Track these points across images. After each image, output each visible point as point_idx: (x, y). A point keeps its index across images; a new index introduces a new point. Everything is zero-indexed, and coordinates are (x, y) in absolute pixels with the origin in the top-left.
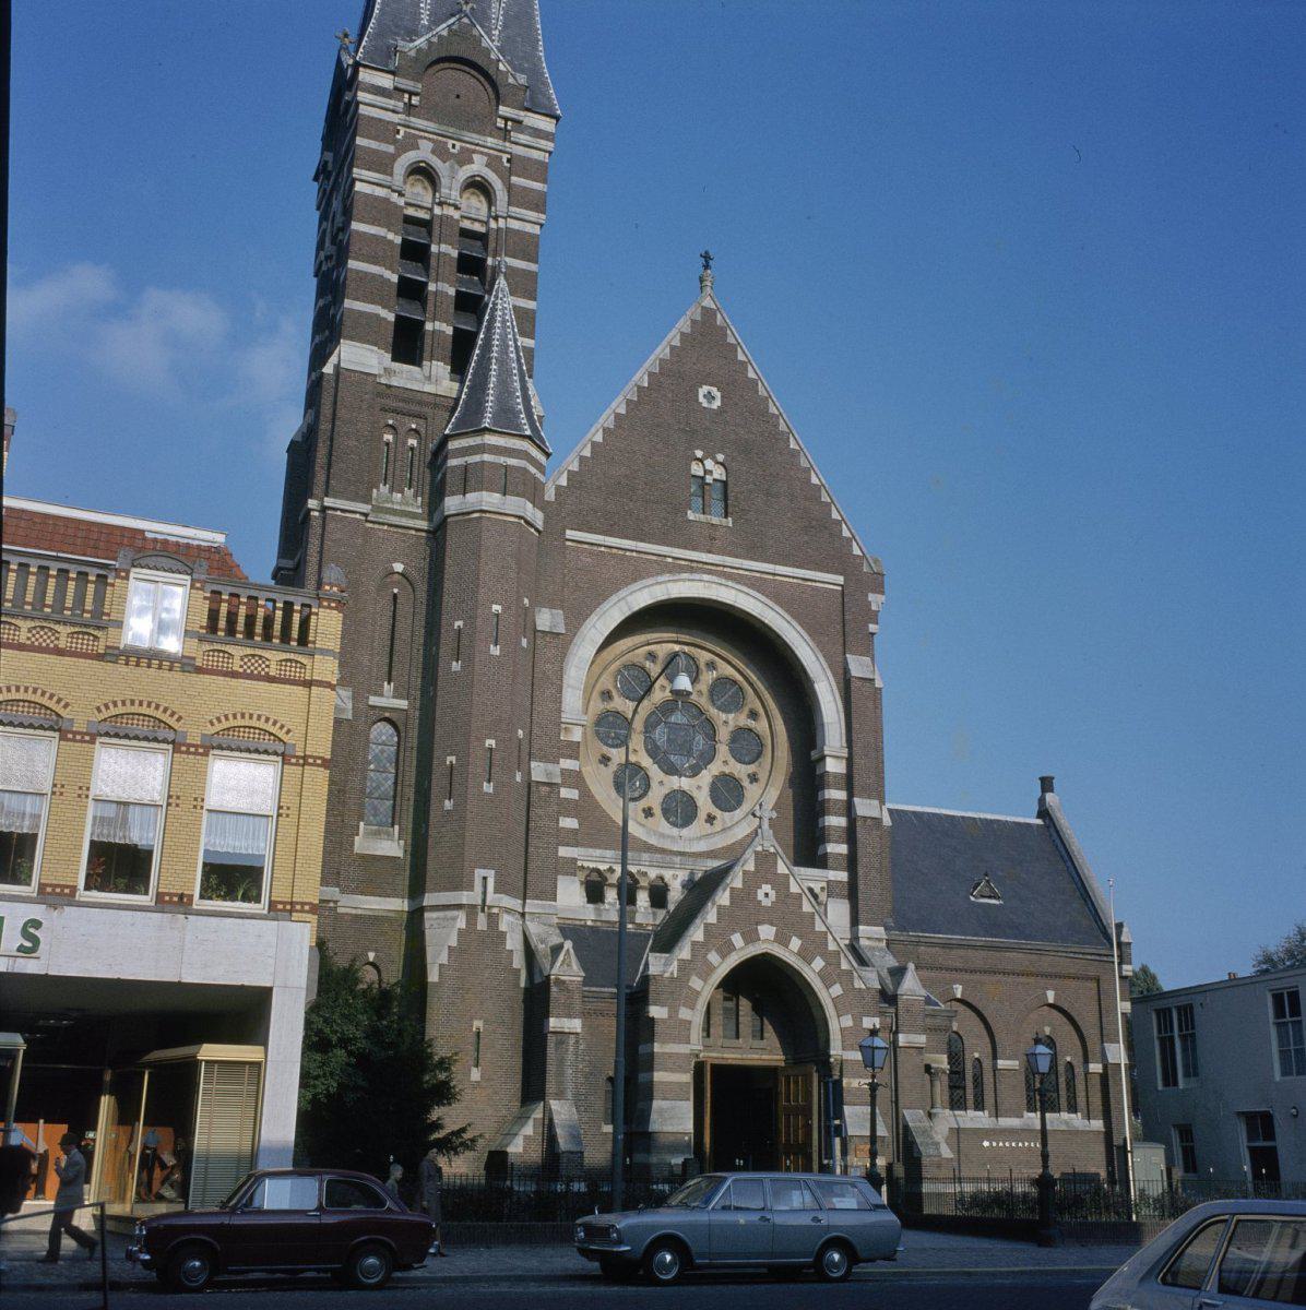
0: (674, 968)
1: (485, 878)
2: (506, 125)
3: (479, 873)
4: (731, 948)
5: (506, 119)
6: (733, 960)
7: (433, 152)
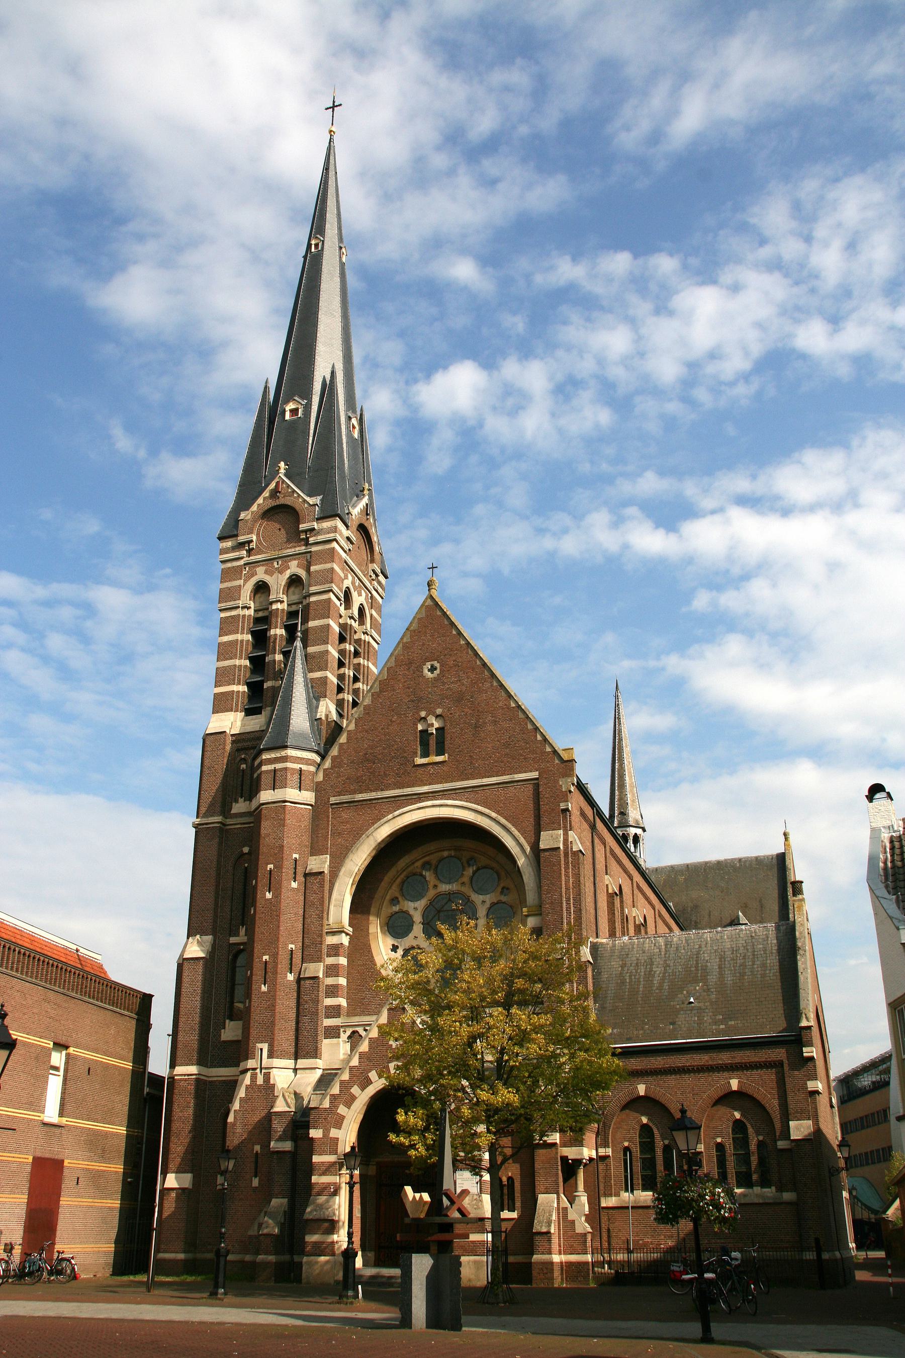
0: (326, 1104)
1: (261, 1050)
2: (306, 535)
3: (259, 1045)
4: (369, 1082)
5: (306, 531)
6: (371, 1090)
7: (266, 572)
